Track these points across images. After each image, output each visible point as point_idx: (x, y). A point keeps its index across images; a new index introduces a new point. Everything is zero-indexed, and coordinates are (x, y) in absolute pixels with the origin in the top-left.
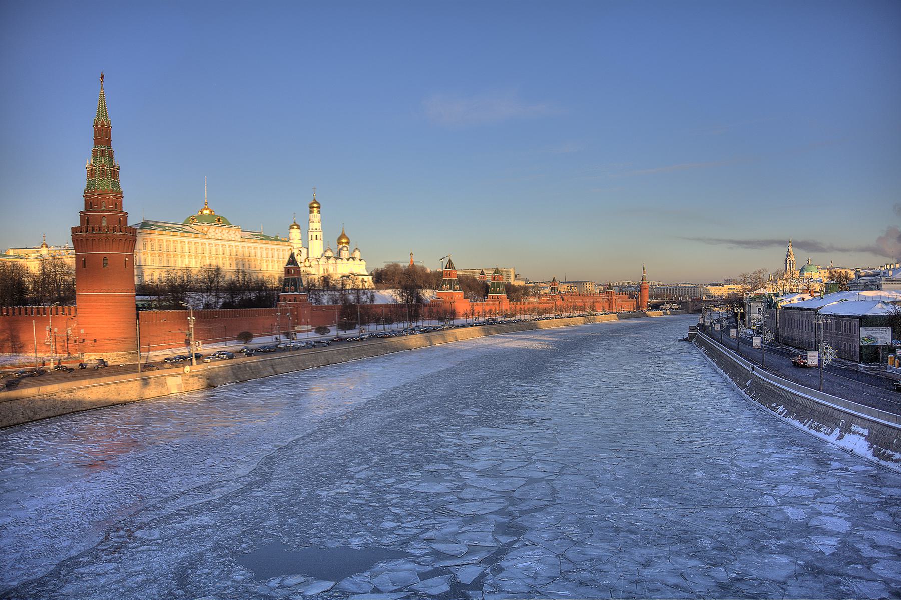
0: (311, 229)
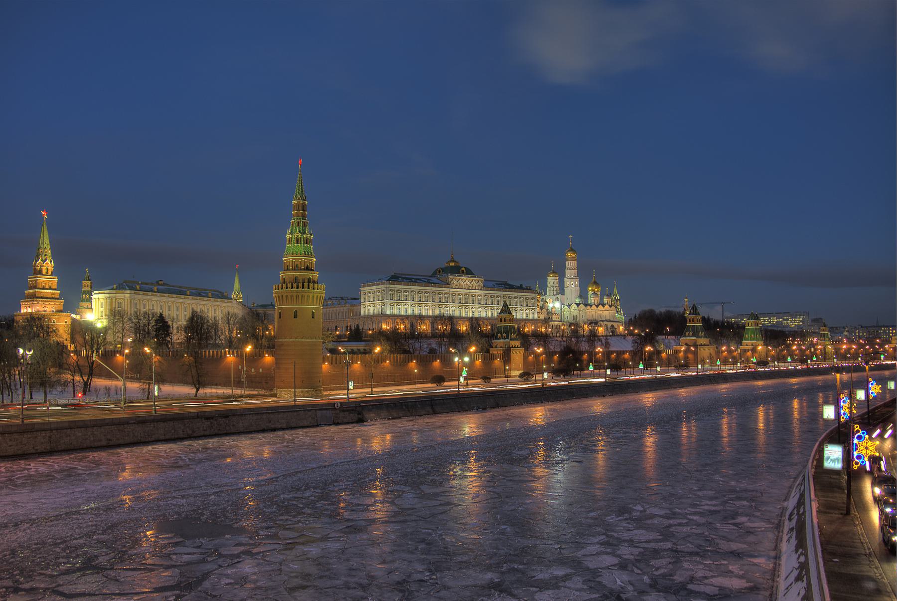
0: (566, 276)
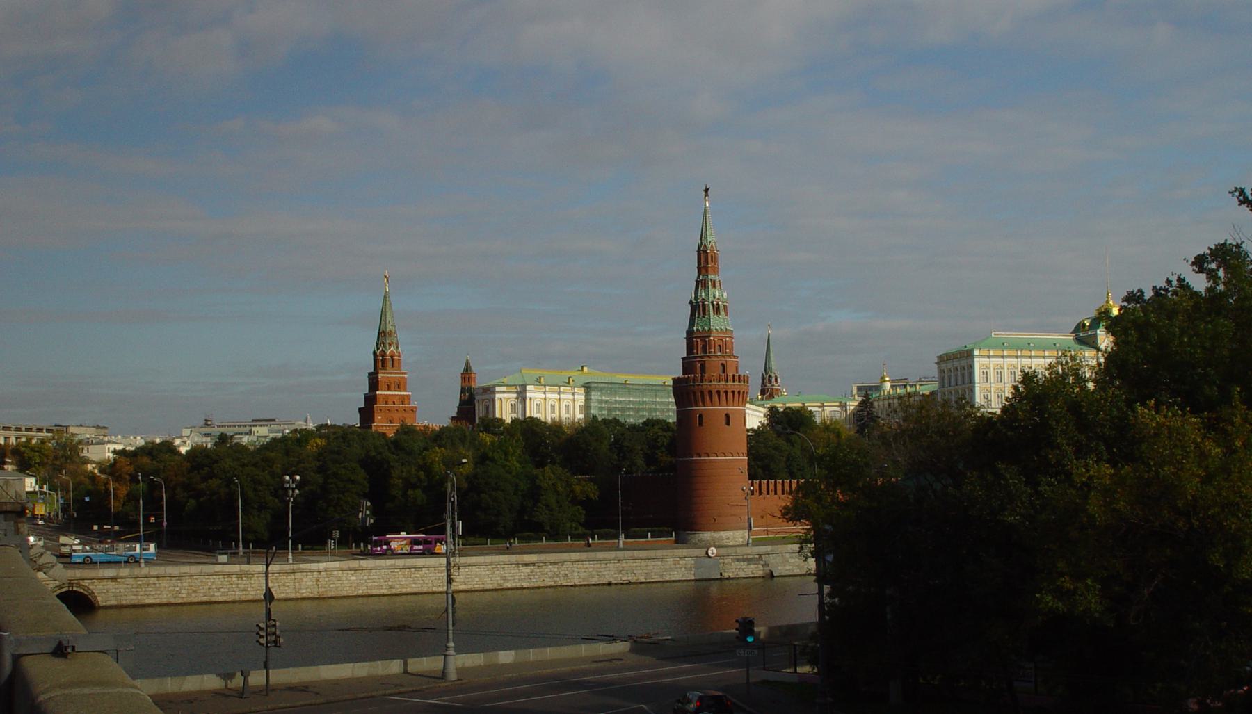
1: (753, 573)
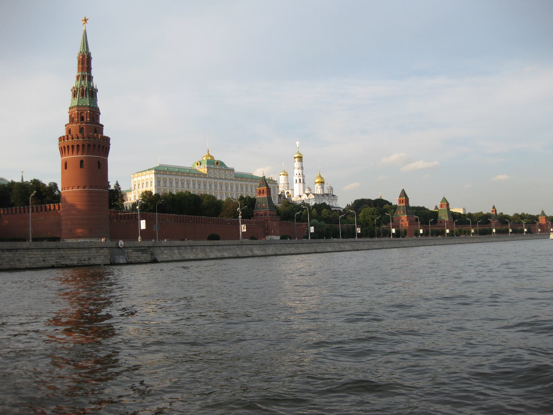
0: (295, 174)
1: (145, 260)
